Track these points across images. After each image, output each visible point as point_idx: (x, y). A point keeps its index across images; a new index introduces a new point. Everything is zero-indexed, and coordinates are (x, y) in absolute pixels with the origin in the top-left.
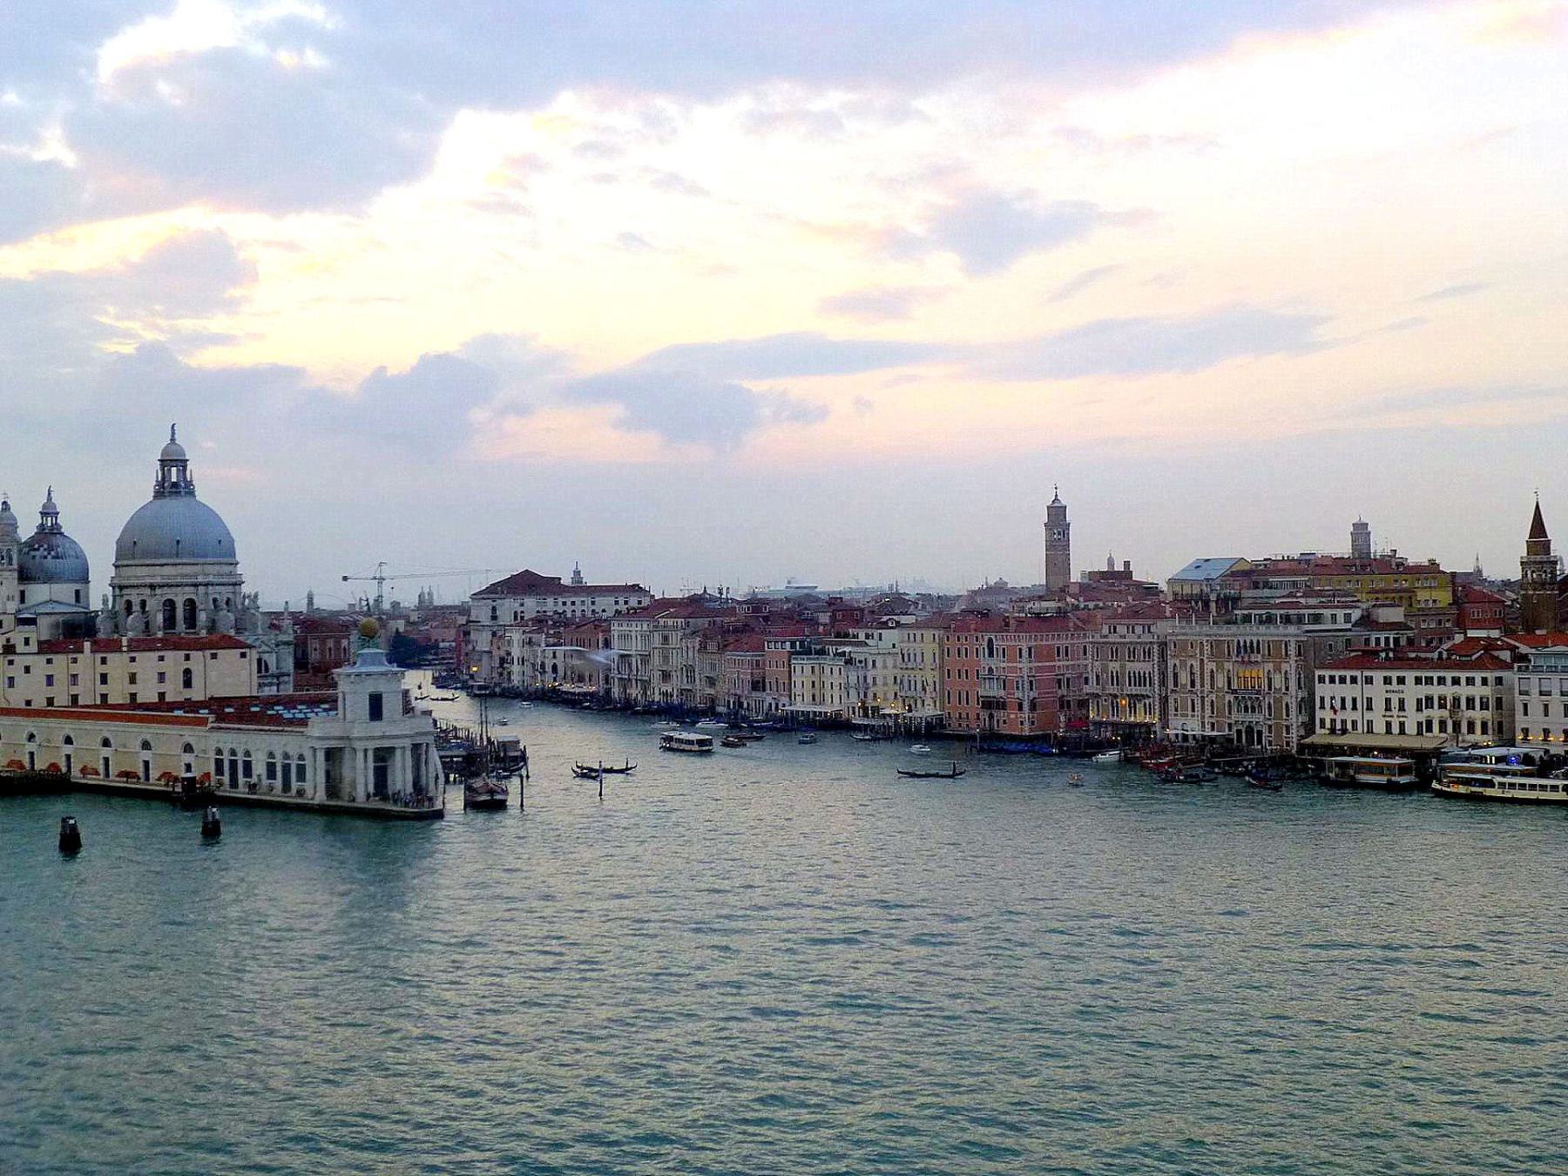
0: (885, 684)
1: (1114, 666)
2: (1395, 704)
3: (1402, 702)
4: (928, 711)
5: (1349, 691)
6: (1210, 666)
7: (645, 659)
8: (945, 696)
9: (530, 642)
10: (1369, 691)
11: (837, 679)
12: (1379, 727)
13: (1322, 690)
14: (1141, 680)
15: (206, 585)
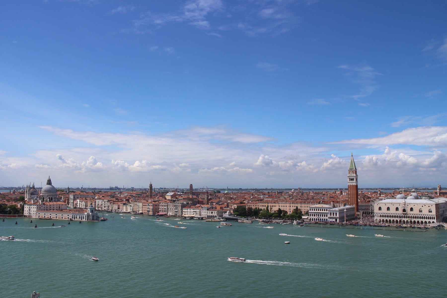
0: (135, 209)
1: (162, 207)
2: (190, 212)
3: (191, 212)
4: (141, 212)
5: (186, 210)
6: (172, 208)
7: (102, 205)
8: (142, 211)
9: (81, 202)
10: (188, 210)
11: (129, 208)
12: (189, 214)
13: (184, 210)
14: (165, 209)
15: (54, 196)
